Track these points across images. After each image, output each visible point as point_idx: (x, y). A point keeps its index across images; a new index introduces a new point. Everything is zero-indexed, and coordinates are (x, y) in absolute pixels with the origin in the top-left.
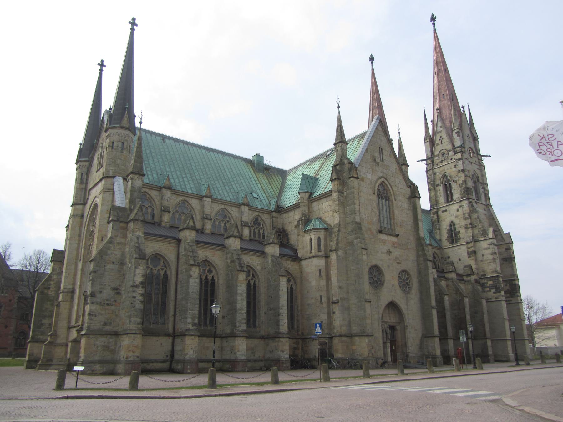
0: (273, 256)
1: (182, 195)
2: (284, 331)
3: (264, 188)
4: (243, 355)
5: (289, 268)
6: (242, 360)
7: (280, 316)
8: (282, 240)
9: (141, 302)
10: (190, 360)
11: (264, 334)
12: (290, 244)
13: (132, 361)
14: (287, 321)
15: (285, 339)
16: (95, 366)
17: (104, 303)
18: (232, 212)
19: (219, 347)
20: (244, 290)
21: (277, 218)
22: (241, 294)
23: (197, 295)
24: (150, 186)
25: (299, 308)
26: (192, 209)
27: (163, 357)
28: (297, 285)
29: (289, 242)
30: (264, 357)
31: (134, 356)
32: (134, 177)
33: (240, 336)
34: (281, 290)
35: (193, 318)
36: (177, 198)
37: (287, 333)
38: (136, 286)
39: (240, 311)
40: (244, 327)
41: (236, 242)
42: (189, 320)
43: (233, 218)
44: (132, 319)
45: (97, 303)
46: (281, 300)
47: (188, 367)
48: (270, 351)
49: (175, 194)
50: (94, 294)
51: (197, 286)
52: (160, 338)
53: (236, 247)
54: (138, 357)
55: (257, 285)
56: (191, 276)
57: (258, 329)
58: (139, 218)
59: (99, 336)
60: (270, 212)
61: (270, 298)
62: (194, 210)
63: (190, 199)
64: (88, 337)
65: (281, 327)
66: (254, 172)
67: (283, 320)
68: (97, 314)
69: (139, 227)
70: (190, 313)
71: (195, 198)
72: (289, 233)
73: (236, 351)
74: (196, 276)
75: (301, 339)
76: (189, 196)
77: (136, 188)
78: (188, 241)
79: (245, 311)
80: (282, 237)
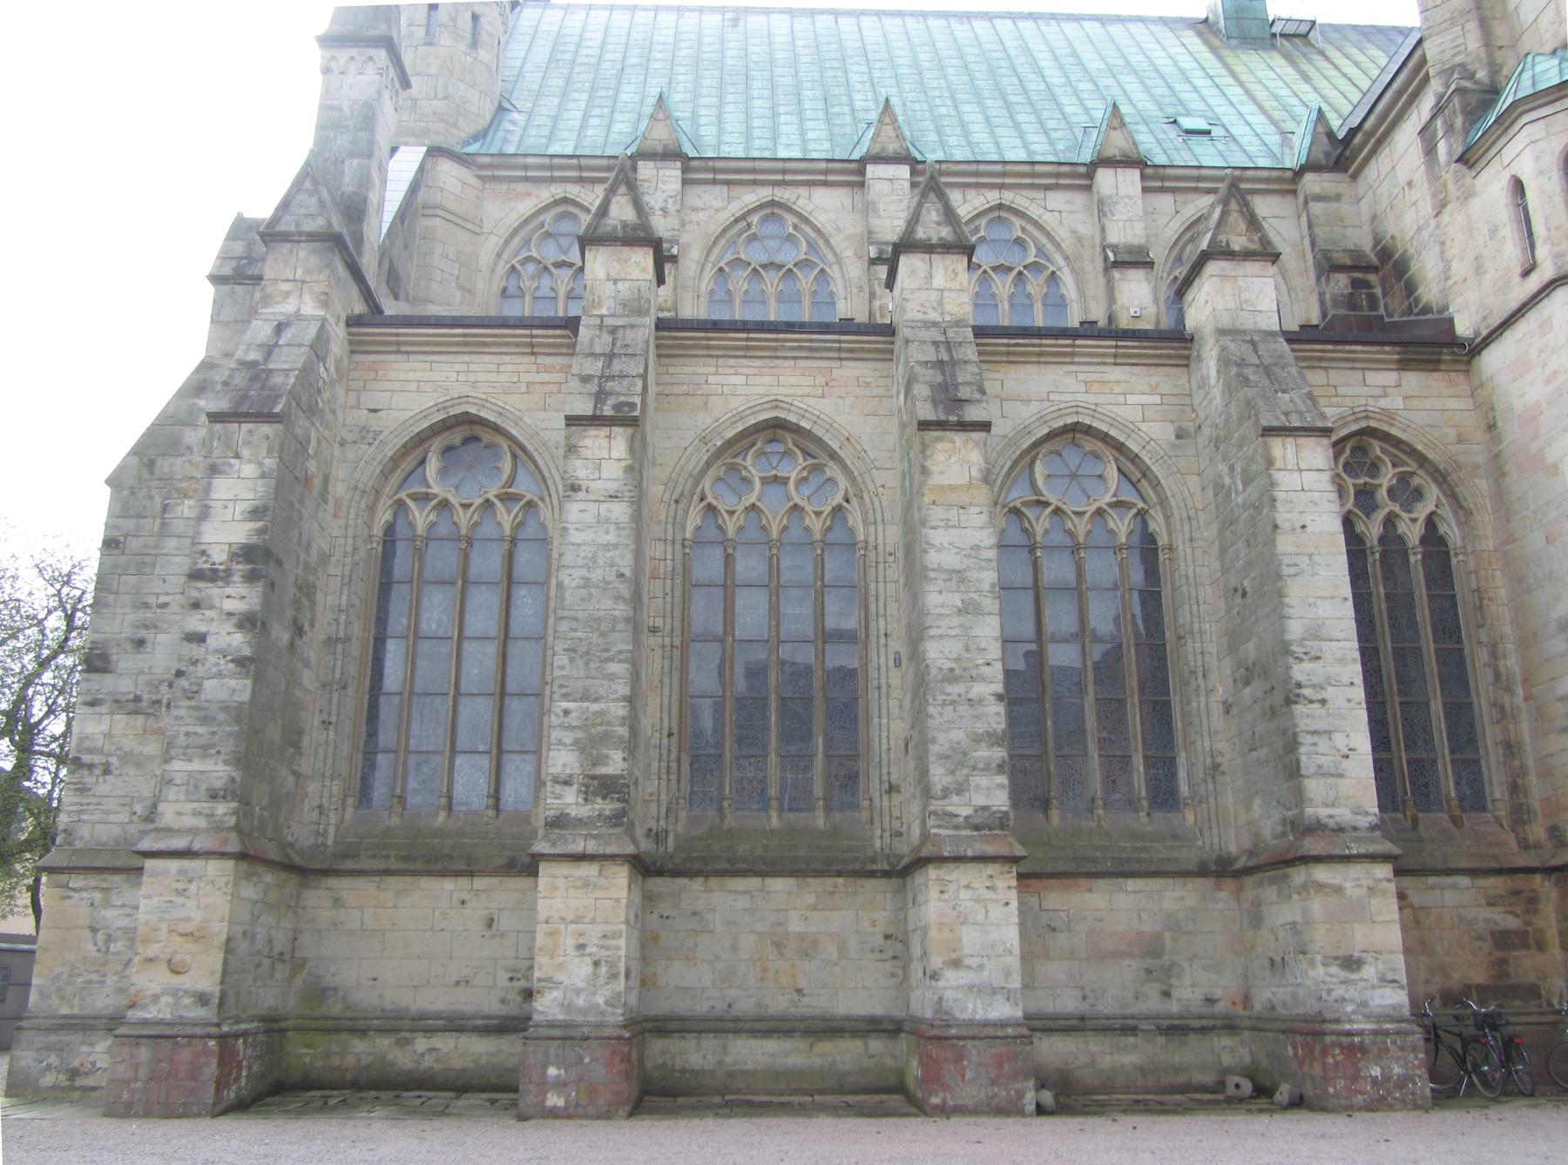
0: (1222, 332)
1: (755, 183)
2: (1343, 814)
3: (1261, 95)
4: (994, 991)
5: (1389, 415)
6: (985, 1024)
7: (1298, 709)
8: (1382, 311)
9: (241, 662)
10: (566, 1025)
11: (1233, 849)
12: (1426, 310)
13: (160, 1022)
14: (1362, 742)
15: (1357, 871)
16: (85, 1049)
17: (158, 702)
18: (1048, 220)
19: (887, 937)
20: (976, 548)
21: (1337, 198)
22: (958, 577)
23: (617, 598)
24: (580, 168)
25: (1511, 663)
26: (821, 242)
27: (503, 1001)
28: (1469, 513)
29: (1417, 300)
30: (1247, 999)
31: (175, 993)
32: (334, 58)
33: (958, 859)
34: (1285, 526)
35: (591, 746)
36: (729, 199)
37: (1373, 828)
38: (213, 576)
39: (950, 689)
40: (992, 793)
41: (939, 280)
42: (562, 760)
43: (1058, 246)
44: (177, 765)
45: (116, 701)
46: (1295, 594)
47: (552, 1071)
48: (1272, 961)
49: (714, 182)
50: (105, 657)
51: (616, 546)
52: (480, 883)
53: (940, 303)
54: (202, 999)
55: (1162, 540)
56: (575, 488)
57: (1190, 817)
58: (298, 225)
59: (118, 878)
60: (1287, 182)
61: (1239, 600)
62: (827, 242)
63: (803, 191)
64: (60, 886)
65: (1314, 787)
66: (1213, 49)
67: (1328, 733)
68: (114, 760)
69: (300, 272)
70: (566, 712)
71: (825, 184)
72: (1412, 251)
73: (936, 962)
74: (613, 486)
75: (1549, 871)
76: (788, 177)
77: (346, 106)
78: (604, 311)
79: (998, 687)
80: (1378, 291)
